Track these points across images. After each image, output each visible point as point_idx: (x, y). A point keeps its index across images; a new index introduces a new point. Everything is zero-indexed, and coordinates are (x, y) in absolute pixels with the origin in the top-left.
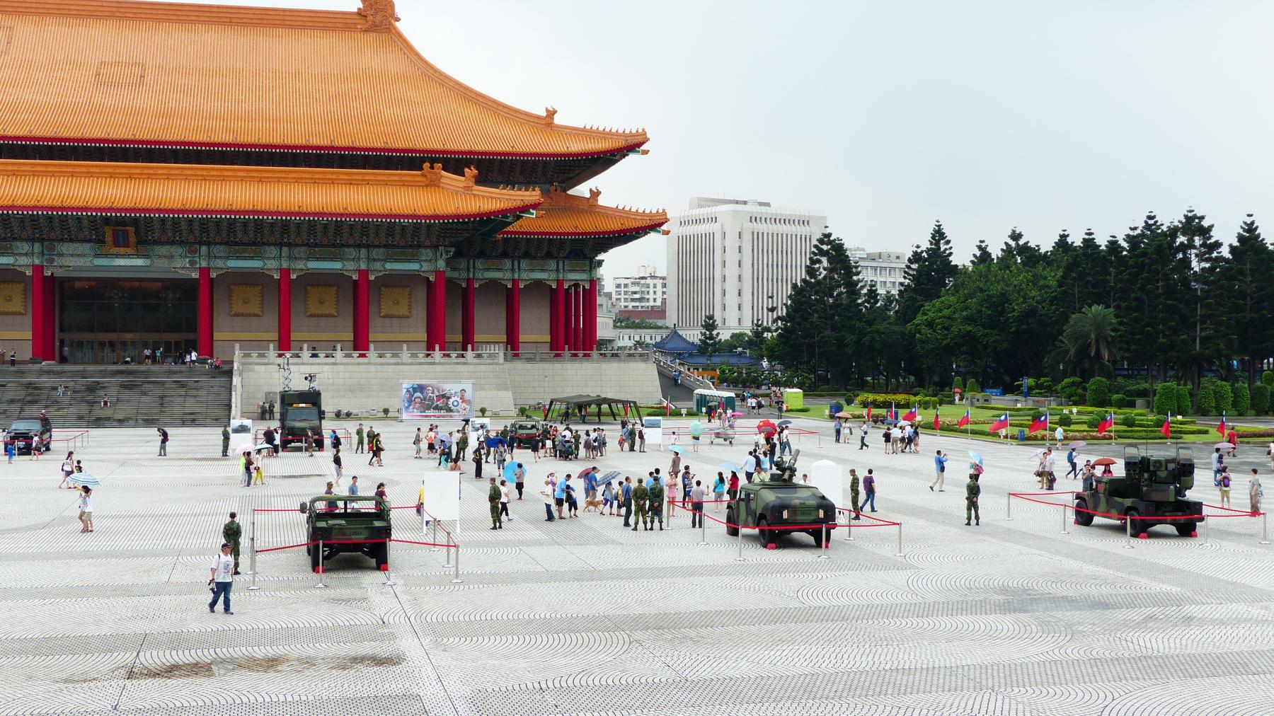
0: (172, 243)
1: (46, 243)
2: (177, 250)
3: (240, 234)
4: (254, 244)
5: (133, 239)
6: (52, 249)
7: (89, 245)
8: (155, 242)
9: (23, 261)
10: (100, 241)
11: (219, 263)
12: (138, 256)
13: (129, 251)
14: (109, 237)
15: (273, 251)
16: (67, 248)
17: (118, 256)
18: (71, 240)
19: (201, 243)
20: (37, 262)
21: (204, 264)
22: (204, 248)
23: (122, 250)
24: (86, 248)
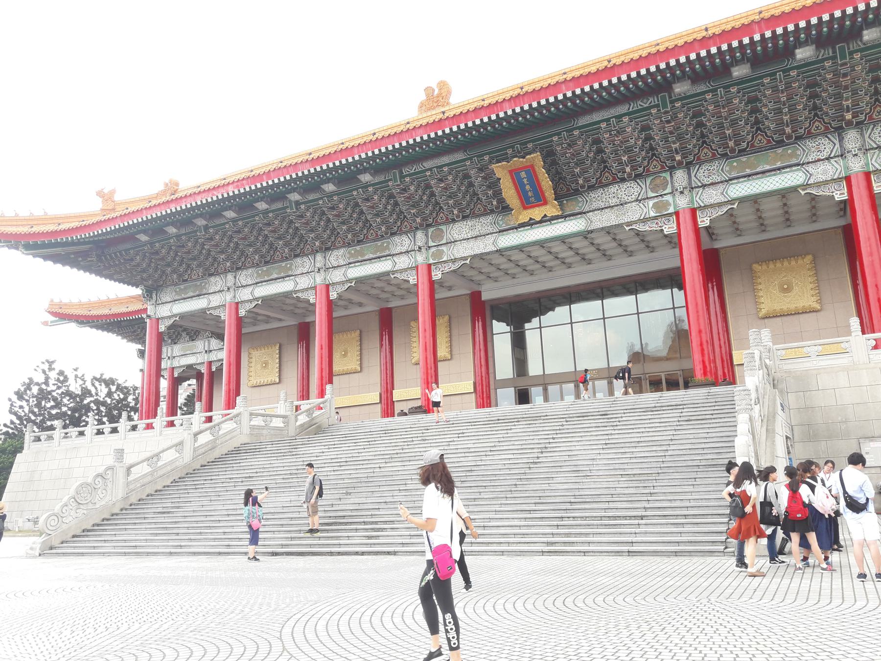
0: (623, 180)
1: (431, 230)
2: (629, 190)
3: (746, 130)
4: (780, 143)
5: (546, 183)
6: (439, 235)
7: (490, 219)
8: (592, 188)
9: (403, 262)
10: (504, 209)
11: (712, 196)
12: (564, 217)
13: (551, 210)
14: (509, 193)
15: (826, 146)
16: (460, 230)
17: (531, 223)
18: (465, 218)
19: (672, 169)
20: (420, 258)
21: (683, 202)
22: (680, 175)
23: (537, 213)
24: (483, 224)
